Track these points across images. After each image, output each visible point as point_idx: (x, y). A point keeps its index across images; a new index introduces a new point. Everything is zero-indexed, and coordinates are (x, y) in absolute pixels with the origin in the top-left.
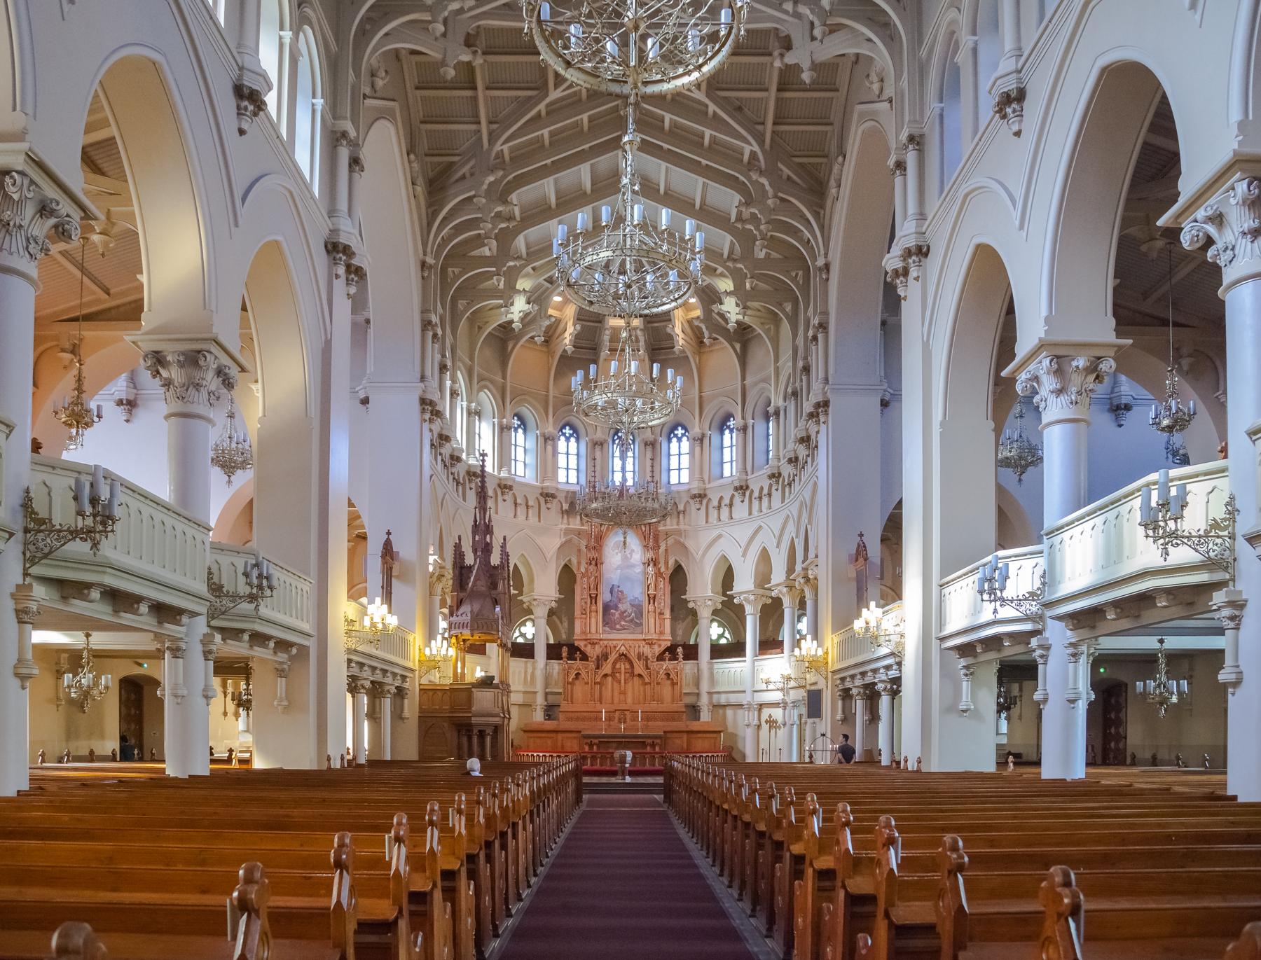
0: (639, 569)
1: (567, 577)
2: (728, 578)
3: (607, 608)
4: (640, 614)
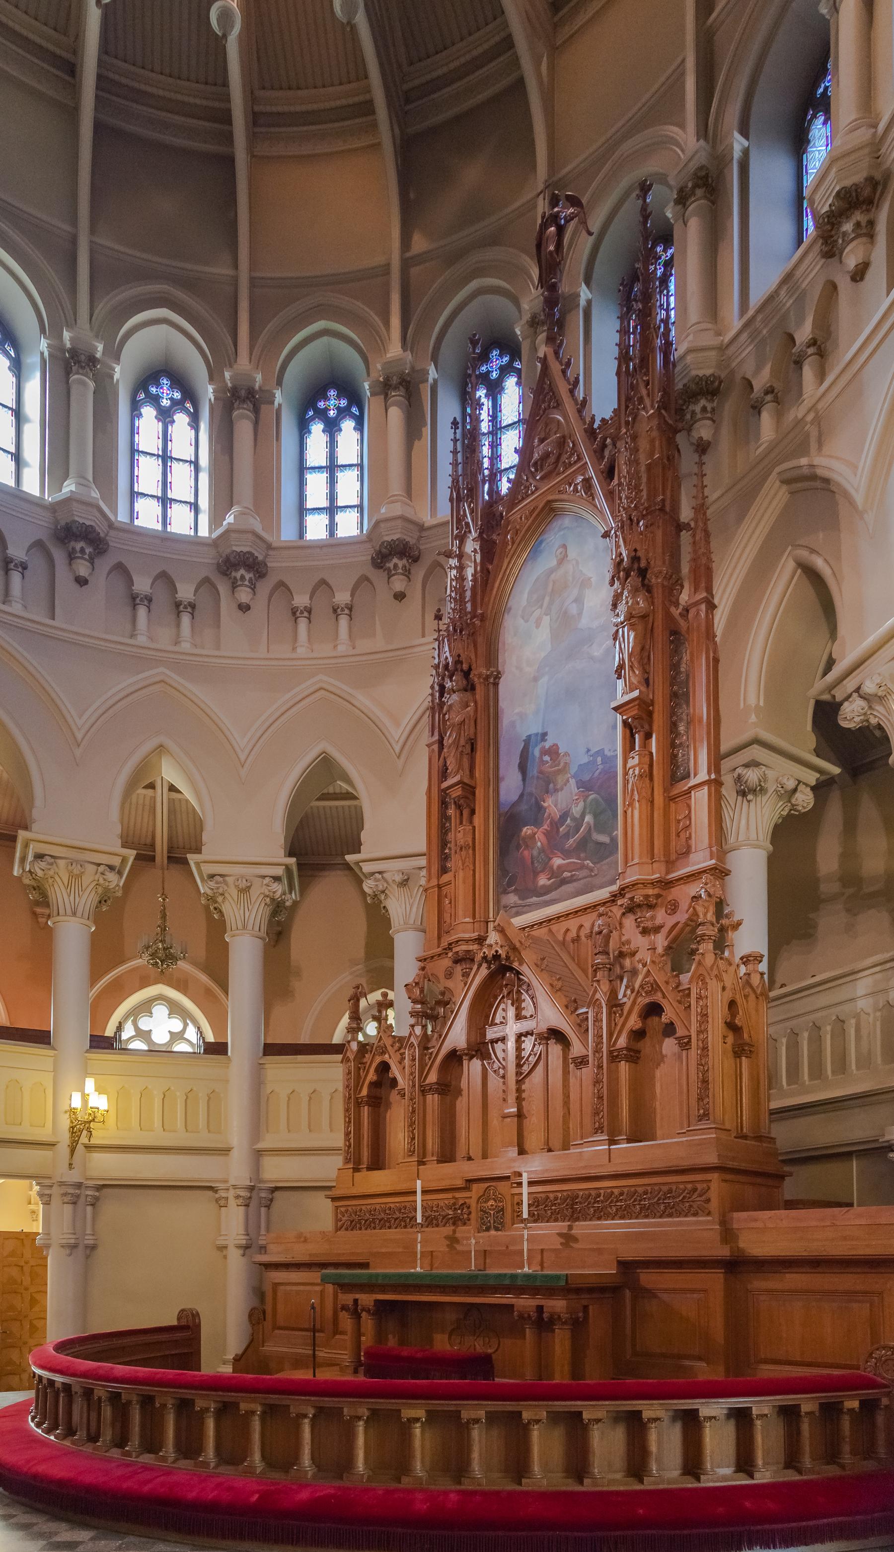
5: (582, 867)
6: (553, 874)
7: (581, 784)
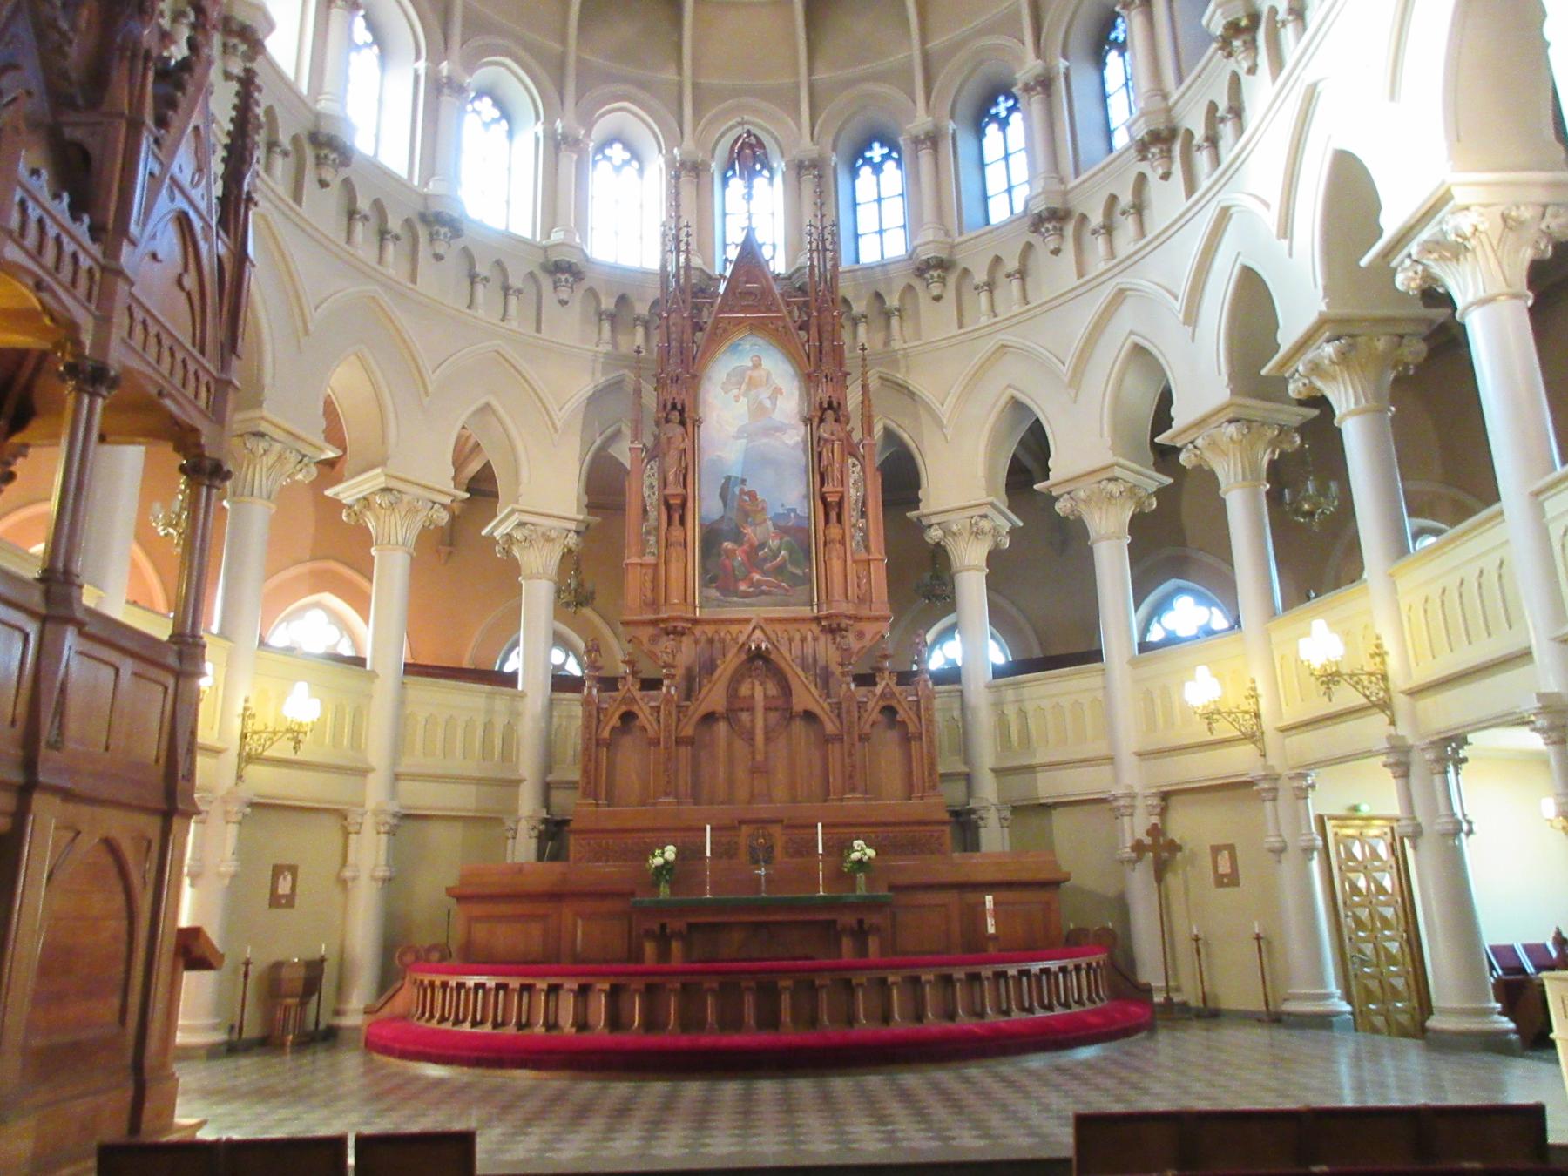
0: (795, 436)
1: (604, 490)
2: (1028, 461)
3: (712, 538)
5: (779, 586)
6: (752, 584)
7: (775, 526)
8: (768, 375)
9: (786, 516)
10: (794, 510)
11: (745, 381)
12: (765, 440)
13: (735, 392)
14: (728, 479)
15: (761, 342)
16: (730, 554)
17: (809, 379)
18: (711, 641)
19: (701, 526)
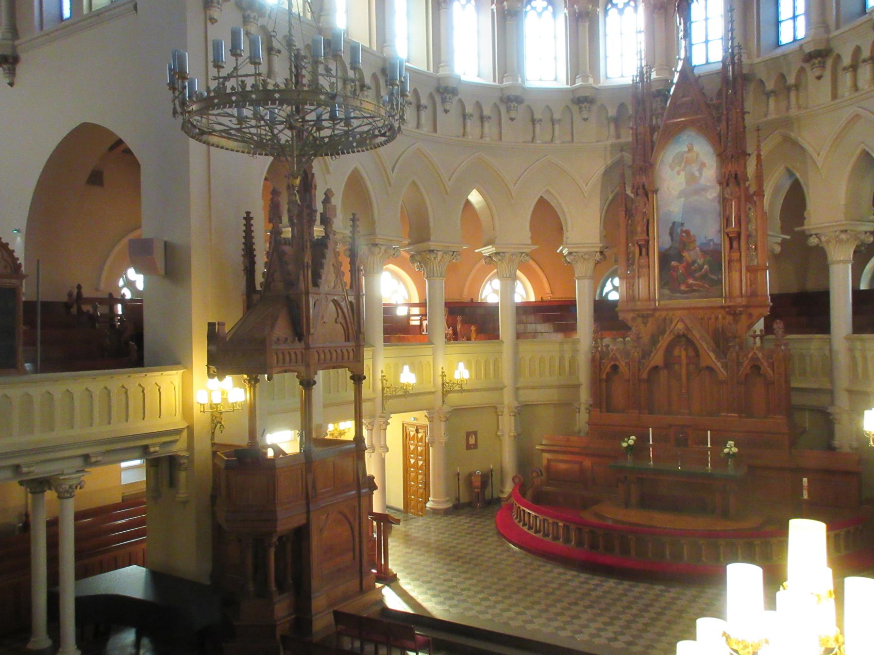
0: (713, 193)
4: (716, 265)
5: (703, 287)
6: (688, 286)
7: (701, 251)
8: (698, 155)
9: (707, 244)
10: (712, 240)
11: (684, 161)
12: (696, 198)
13: (678, 168)
14: (674, 223)
15: (693, 133)
16: (675, 269)
17: (722, 157)
18: (665, 319)
19: (659, 253)
